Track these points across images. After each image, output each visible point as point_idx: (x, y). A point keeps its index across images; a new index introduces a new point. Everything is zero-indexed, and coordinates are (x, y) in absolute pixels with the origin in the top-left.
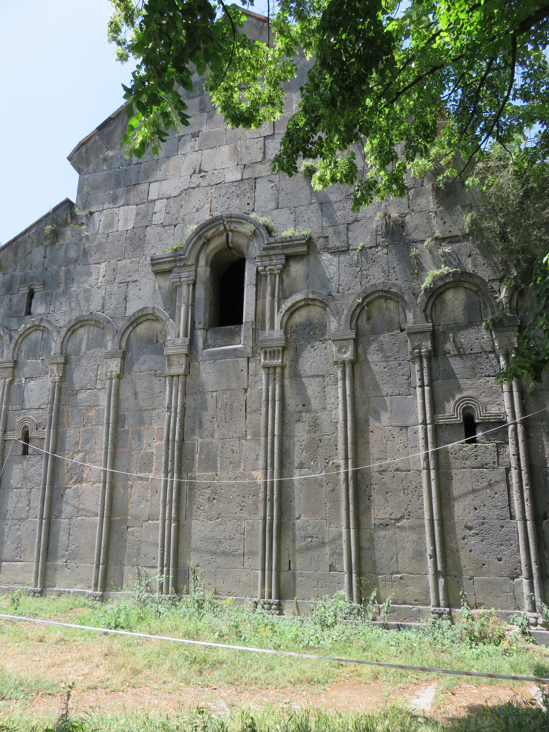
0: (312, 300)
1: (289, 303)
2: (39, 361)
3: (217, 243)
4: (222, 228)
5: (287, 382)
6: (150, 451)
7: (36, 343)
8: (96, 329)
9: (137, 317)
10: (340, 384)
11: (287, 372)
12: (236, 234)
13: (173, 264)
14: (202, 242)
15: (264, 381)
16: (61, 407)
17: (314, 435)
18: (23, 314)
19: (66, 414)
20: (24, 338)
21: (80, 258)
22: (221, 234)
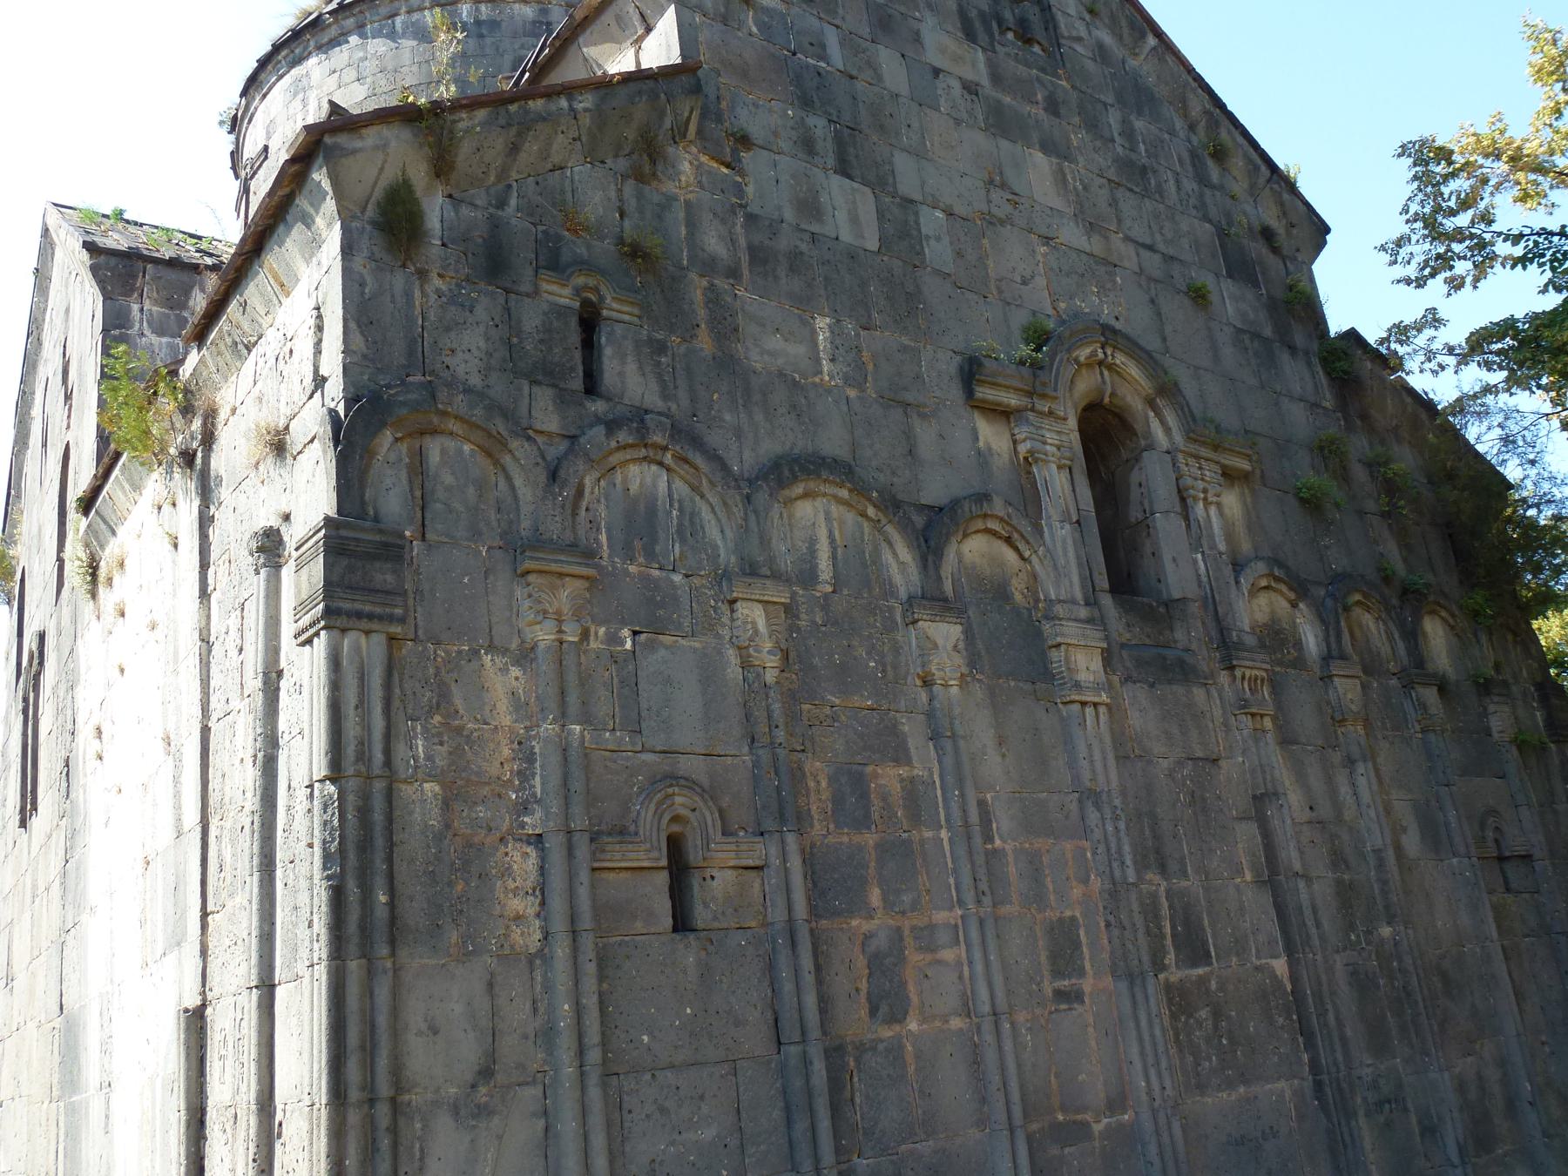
2: (677, 578)
6: (1068, 913)
7: (652, 510)
8: (850, 517)
18: (577, 383)
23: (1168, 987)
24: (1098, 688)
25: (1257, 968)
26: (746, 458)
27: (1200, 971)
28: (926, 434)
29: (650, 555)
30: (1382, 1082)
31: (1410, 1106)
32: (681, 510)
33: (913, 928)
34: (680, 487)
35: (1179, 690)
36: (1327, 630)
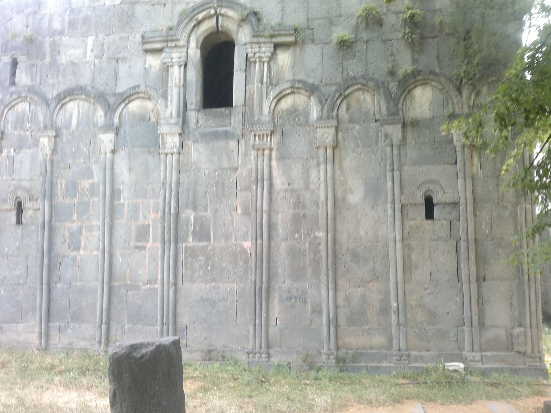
0: (298, 88)
1: (278, 90)
3: (208, 26)
4: (212, 12)
5: (274, 163)
6: (146, 223)
7: (24, 115)
8: (86, 104)
9: (128, 94)
10: (322, 167)
11: (274, 154)
12: (225, 19)
13: (164, 44)
14: (193, 25)
15: (253, 162)
16: (54, 180)
17: (297, 211)
18: (7, 83)
19: (59, 187)
20: (10, 109)
21: (66, 31)
22: (209, 17)
23: (187, 248)
24: (172, 148)
25: (234, 244)
26: (51, 94)
27: (204, 244)
28: (123, 69)
29: (22, 128)
30: (293, 291)
31: (309, 301)
32: (32, 113)
33: (85, 226)
34: (33, 107)
35: (222, 143)
36: (323, 108)
